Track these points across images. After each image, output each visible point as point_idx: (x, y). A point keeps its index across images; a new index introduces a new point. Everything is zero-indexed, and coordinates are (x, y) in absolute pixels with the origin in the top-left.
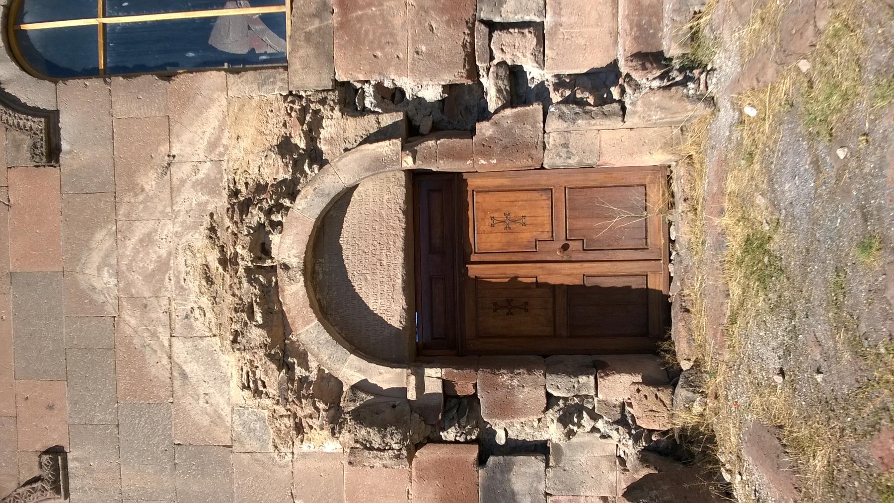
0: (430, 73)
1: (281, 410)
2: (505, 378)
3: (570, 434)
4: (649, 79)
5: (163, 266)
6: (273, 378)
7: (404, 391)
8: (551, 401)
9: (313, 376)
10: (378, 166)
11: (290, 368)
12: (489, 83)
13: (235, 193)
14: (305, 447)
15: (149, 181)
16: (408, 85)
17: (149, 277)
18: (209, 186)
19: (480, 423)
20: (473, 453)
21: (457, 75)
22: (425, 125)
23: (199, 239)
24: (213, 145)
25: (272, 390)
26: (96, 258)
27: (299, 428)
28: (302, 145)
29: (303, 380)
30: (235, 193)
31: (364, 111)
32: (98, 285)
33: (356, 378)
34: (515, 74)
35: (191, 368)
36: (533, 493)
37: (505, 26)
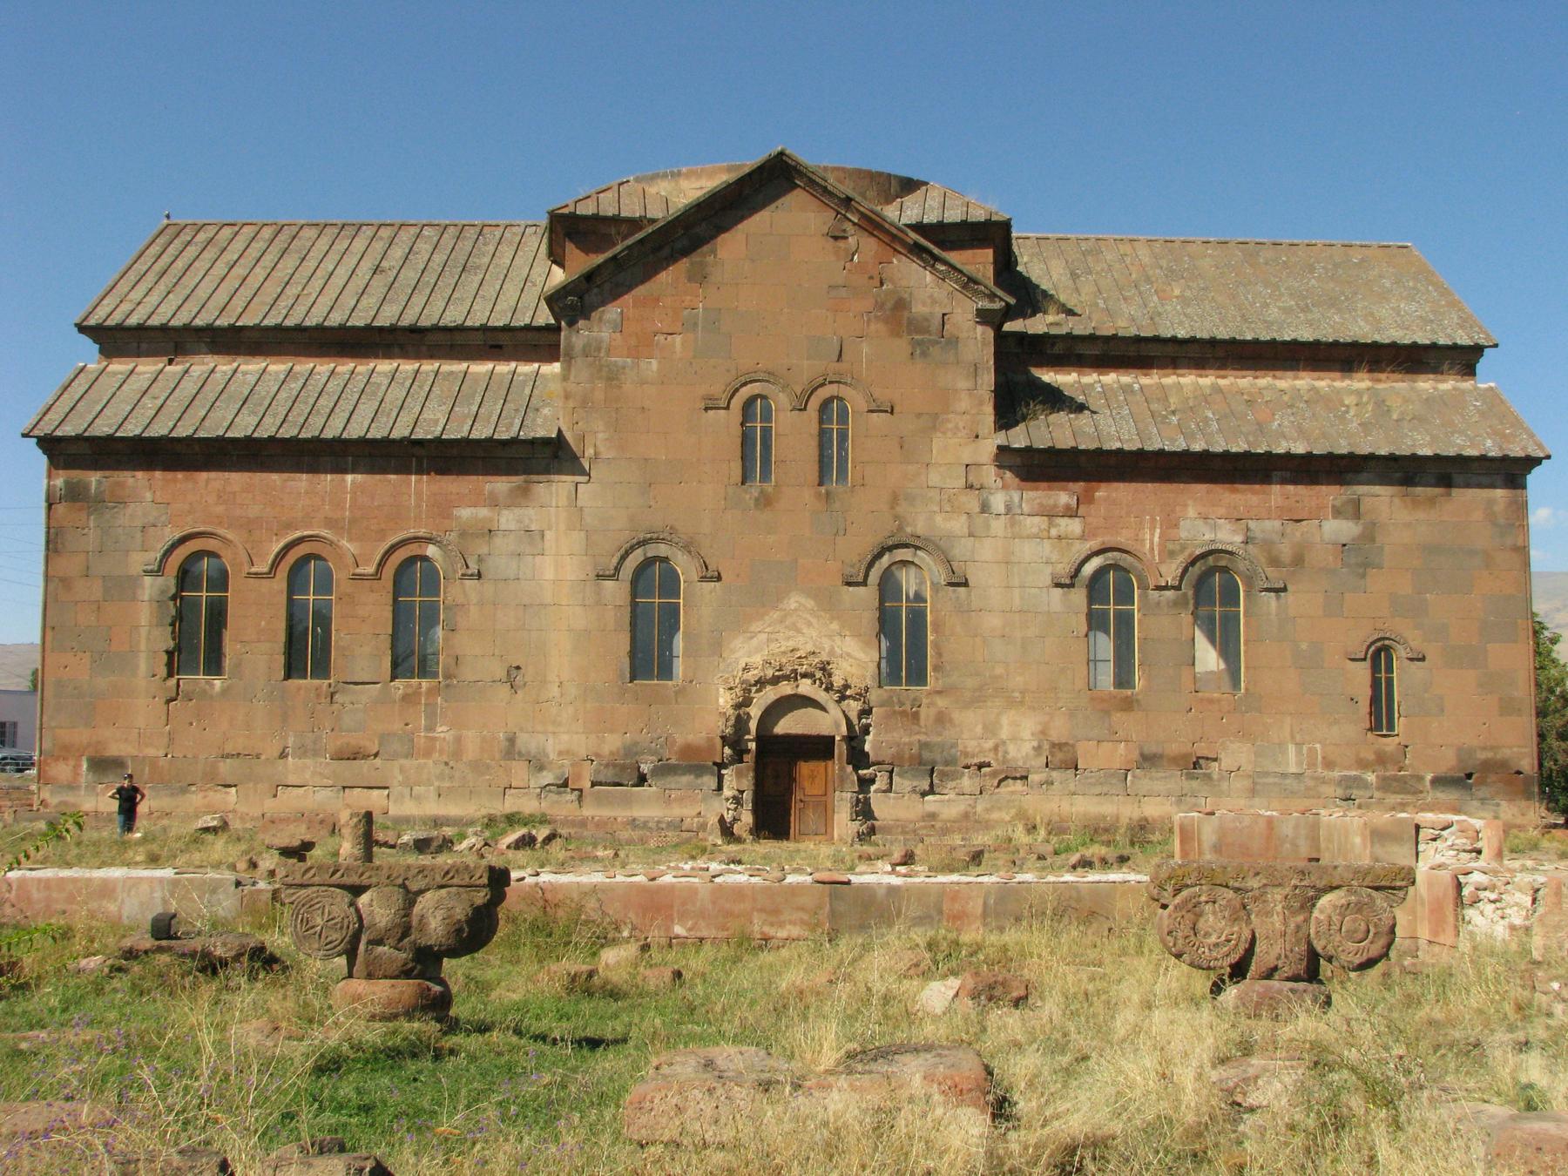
0: (873, 747)
1: (737, 681)
2: (751, 774)
3: (727, 799)
4: (864, 828)
5: (799, 631)
6: (752, 676)
7: (749, 733)
8: (742, 792)
9: (752, 695)
10: (838, 726)
11: (755, 685)
12: (871, 770)
13: (828, 663)
14: (721, 690)
15: (835, 626)
16: (869, 738)
17: (794, 624)
18: (832, 652)
19: (731, 763)
20: (719, 761)
21: (872, 758)
22: (854, 744)
23: (810, 648)
24: (848, 655)
25: (745, 677)
26: (803, 600)
27: (731, 689)
28: (848, 693)
29: (750, 691)
30: (828, 663)
31: (860, 719)
32: (792, 600)
33: (752, 714)
34: (872, 781)
35: (755, 642)
36: (703, 784)
37: (891, 778)
